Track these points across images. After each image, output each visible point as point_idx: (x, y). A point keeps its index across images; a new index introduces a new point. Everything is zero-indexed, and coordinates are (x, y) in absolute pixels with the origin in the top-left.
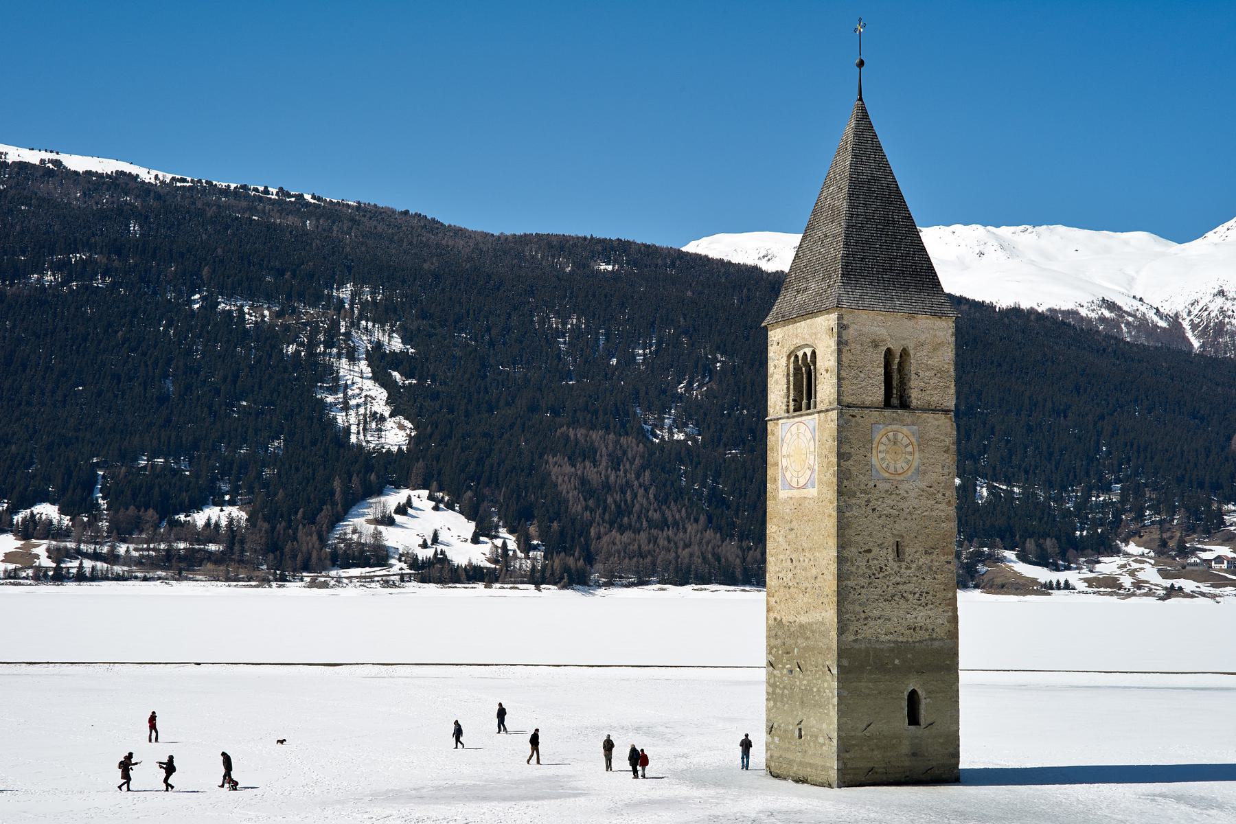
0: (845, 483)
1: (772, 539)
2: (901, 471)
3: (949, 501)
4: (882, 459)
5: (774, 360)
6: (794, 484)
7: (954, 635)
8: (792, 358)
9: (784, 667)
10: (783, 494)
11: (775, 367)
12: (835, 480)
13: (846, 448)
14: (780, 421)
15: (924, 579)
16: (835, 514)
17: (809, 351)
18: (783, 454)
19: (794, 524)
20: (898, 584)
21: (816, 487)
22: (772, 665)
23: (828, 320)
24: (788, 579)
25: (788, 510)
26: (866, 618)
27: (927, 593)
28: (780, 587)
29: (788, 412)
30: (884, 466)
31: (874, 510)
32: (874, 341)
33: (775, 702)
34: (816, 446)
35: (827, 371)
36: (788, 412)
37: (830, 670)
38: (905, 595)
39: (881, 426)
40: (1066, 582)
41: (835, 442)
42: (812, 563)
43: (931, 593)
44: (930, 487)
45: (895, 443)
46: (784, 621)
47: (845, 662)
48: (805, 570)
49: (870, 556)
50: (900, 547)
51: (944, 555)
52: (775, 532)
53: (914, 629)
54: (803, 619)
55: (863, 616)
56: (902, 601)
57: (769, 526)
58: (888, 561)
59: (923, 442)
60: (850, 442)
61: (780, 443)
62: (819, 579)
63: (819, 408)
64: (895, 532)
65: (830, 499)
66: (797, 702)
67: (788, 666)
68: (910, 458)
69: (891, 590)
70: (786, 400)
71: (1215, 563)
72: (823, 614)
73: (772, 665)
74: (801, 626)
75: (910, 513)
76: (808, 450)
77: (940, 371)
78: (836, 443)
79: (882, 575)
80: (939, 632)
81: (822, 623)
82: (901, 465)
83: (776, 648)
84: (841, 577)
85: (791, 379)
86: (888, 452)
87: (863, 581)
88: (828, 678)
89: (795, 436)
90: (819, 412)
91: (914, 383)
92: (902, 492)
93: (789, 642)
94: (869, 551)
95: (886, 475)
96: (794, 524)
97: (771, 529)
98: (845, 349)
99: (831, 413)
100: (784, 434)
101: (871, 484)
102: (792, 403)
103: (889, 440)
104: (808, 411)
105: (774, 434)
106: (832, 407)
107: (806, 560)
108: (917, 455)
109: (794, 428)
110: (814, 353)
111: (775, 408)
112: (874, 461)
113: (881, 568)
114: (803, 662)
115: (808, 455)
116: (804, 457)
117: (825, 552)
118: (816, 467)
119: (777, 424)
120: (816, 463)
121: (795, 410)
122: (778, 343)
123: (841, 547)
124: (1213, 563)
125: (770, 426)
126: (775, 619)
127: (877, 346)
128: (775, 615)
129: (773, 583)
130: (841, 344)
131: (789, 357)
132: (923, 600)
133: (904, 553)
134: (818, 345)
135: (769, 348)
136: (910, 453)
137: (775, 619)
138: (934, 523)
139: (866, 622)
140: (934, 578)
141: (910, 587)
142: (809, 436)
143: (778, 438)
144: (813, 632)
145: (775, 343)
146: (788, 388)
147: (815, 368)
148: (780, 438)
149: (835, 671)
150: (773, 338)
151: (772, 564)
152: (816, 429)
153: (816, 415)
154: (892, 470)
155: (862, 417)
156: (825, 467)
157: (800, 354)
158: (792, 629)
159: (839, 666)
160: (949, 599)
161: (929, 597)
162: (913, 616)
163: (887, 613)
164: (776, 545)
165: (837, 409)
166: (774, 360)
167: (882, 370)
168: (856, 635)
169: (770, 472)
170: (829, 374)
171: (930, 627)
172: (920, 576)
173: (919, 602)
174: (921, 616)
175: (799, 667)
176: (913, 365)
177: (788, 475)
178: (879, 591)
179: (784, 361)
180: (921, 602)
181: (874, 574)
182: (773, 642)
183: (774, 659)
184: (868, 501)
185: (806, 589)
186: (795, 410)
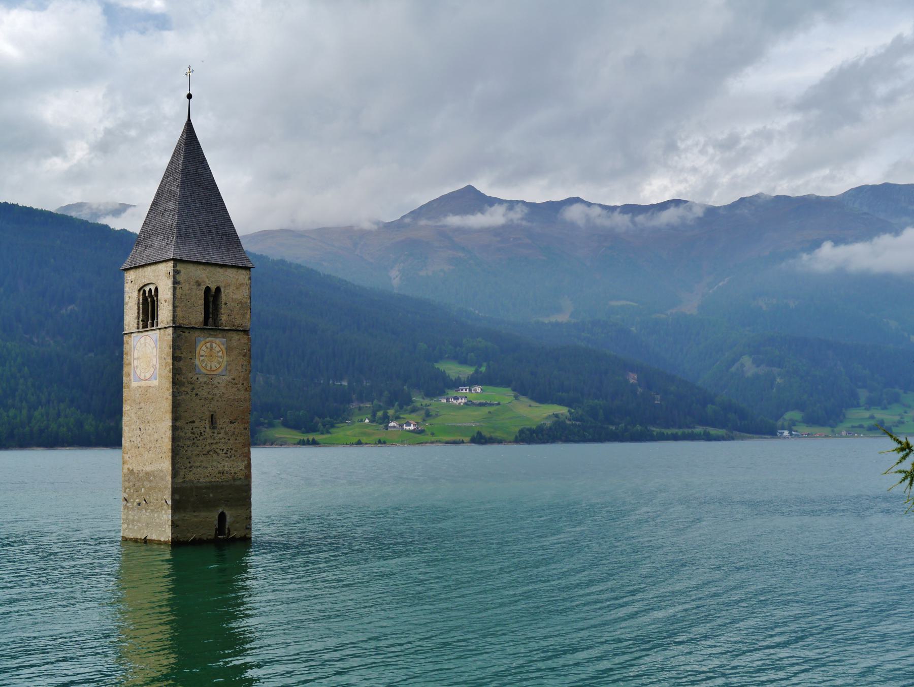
0: (178, 376)
2: (215, 369)
3: (246, 388)
4: (203, 361)
5: (129, 293)
6: (142, 378)
7: (248, 477)
8: (141, 292)
9: (134, 502)
10: (134, 384)
11: (130, 297)
12: (171, 375)
13: (178, 354)
14: (133, 334)
15: (229, 440)
16: (170, 397)
18: (135, 357)
19: (142, 405)
20: (212, 443)
22: (126, 500)
24: (138, 442)
25: (138, 395)
26: (191, 467)
27: (231, 449)
28: (132, 447)
29: (138, 328)
30: (204, 365)
31: (197, 394)
32: (197, 282)
33: (128, 525)
35: (166, 301)
36: (138, 328)
37: (166, 502)
38: (216, 450)
39: (202, 339)
40: (313, 440)
41: (170, 349)
42: (154, 430)
43: (234, 449)
44: (234, 379)
45: (211, 350)
46: (135, 470)
47: (177, 497)
48: (150, 435)
49: (195, 425)
50: (214, 419)
51: (242, 424)
53: (223, 473)
54: (148, 468)
55: (189, 465)
56: (215, 456)
57: (124, 406)
58: (206, 428)
59: (229, 349)
60: (181, 349)
62: (159, 441)
63: (159, 326)
64: (211, 409)
66: (143, 523)
67: (137, 500)
68: (221, 360)
69: (208, 448)
70: (137, 320)
71: (406, 426)
73: (126, 500)
74: (147, 473)
75: (221, 397)
77: (241, 303)
78: (171, 350)
79: (202, 438)
80: (240, 475)
81: (161, 471)
82: (214, 365)
84: (174, 439)
85: (141, 306)
86: (206, 356)
87: (189, 443)
88: (165, 507)
90: (160, 329)
91: (223, 310)
92: (215, 382)
94: (194, 422)
95: (205, 372)
96: (142, 405)
97: (126, 408)
98: (178, 287)
99: (168, 330)
100: (135, 343)
101: (195, 378)
102: (141, 323)
103: (207, 348)
104: (153, 328)
105: (128, 344)
106: (169, 325)
107: (150, 428)
108: (225, 358)
109: (142, 340)
110: (156, 289)
111: (129, 326)
112: (197, 362)
113: (201, 433)
114: (148, 497)
116: (149, 359)
118: (158, 366)
119: (130, 337)
120: (158, 363)
121: (143, 328)
122: (132, 282)
123: (175, 419)
124: (405, 425)
125: (126, 338)
126: (128, 469)
127: (199, 285)
128: (128, 466)
129: (127, 445)
130: (175, 283)
131: (139, 291)
132: (229, 454)
133: (216, 423)
135: (126, 285)
136: (221, 357)
137: (128, 469)
138: (236, 404)
139: (191, 469)
140: (236, 439)
141: (222, 446)
142: (153, 345)
144: (155, 477)
145: (129, 282)
146: (138, 313)
147: (157, 299)
148: (132, 347)
149: (170, 503)
151: (127, 431)
152: (158, 340)
153: (158, 331)
154: (208, 368)
155: (189, 333)
156: (164, 365)
157: (147, 289)
158: (140, 475)
159: (172, 499)
160: (246, 453)
161: (233, 452)
162: (222, 465)
163: (204, 464)
165: (173, 327)
166: (129, 293)
167: (202, 302)
168: (184, 478)
169: (125, 369)
170: (167, 303)
171: (233, 471)
172: (227, 438)
173: (226, 455)
174: (226, 465)
175: (145, 501)
176: (223, 297)
177: (138, 372)
178: (199, 449)
179: (135, 294)
180: (227, 455)
181: (196, 437)
182: (127, 484)
183: (127, 496)
184: (193, 389)
186: (143, 328)
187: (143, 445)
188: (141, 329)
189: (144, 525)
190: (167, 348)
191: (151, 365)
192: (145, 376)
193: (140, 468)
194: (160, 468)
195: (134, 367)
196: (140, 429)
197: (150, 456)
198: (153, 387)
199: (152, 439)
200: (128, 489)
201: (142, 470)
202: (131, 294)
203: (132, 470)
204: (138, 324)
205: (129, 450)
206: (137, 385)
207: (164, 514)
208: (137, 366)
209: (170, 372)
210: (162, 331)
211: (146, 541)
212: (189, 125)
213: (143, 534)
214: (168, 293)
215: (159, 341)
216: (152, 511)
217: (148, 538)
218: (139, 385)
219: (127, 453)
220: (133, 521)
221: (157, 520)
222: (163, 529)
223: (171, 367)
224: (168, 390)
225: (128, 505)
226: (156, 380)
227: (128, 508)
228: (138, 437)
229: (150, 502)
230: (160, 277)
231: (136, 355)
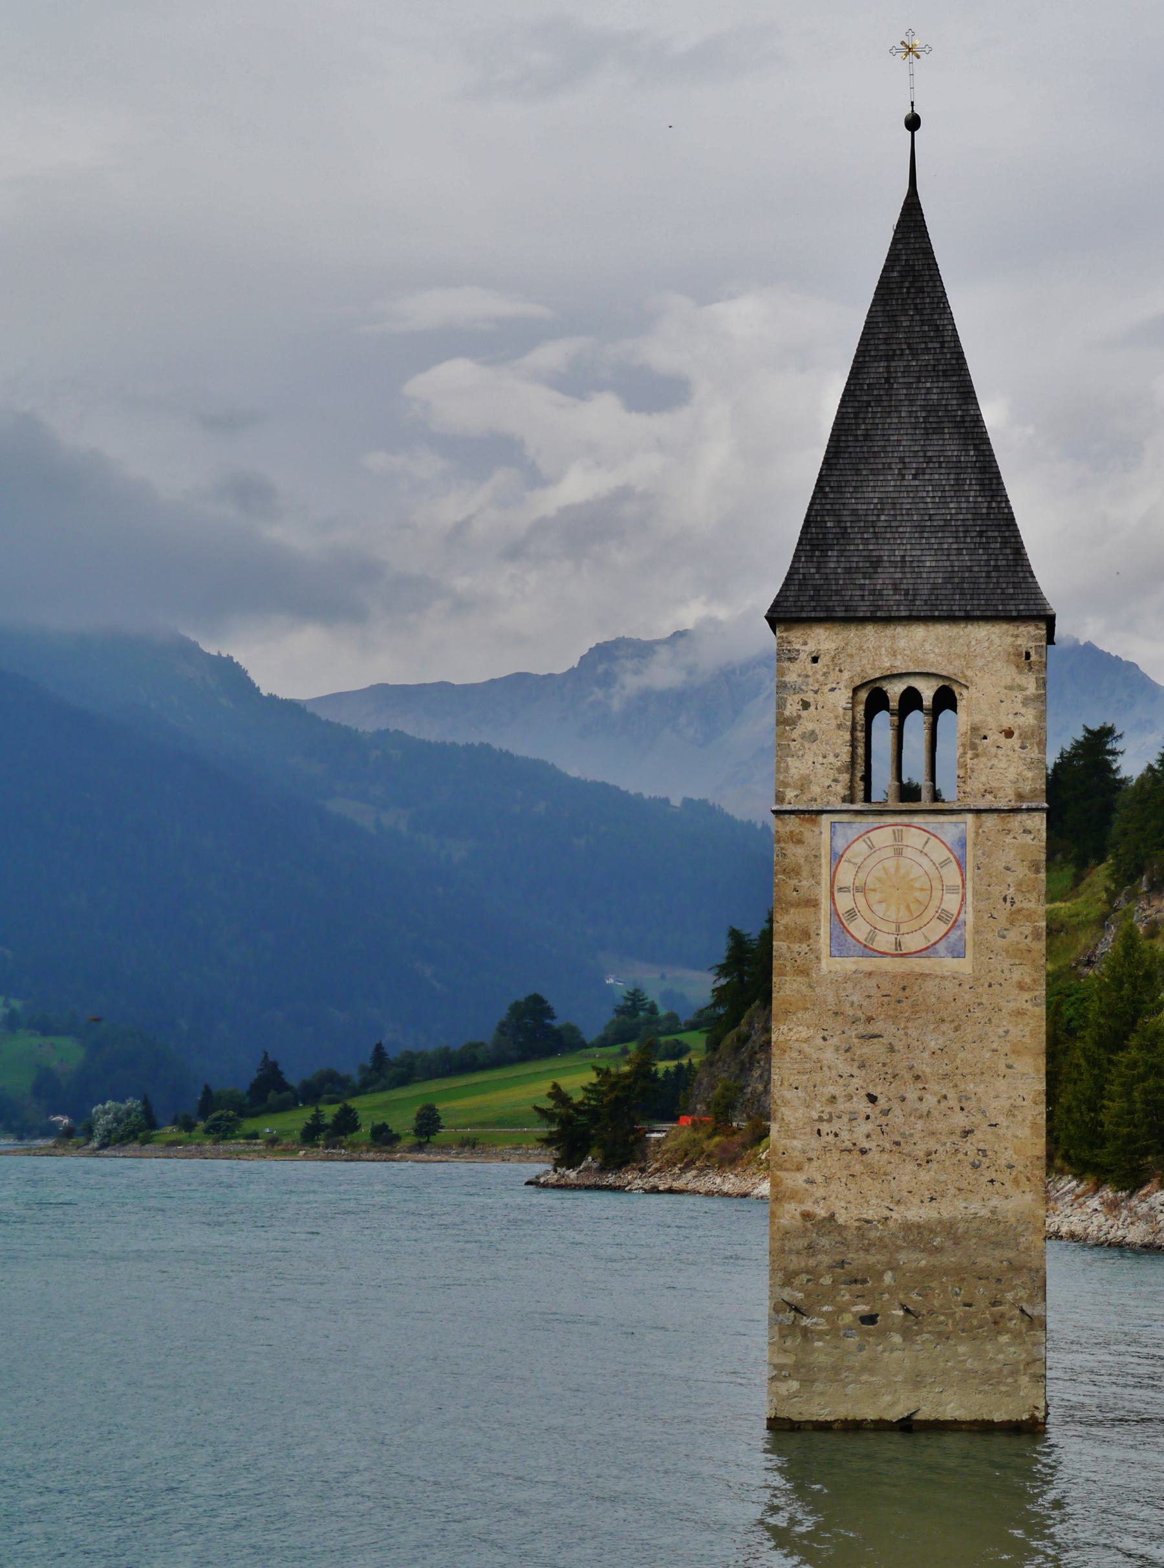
1: (794, 1055)
6: (884, 942)
8: (863, 695)
9: (841, 1310)
10: (829, 965)
11: (806, 705)
14: (824, 816)
16: (1041, 1011)
17: (927, 691)
18: (837, 885)
21: (969, 952)
23: (1017, 636)
28: (826, 1149)
33: (807, 1382)
34: (969, 875)
41: (1037, 871)
52: (806, 1040)
54: (916, 1213)
61: (825, 861)
62: (978, 1134)
65: (1020, 983)
67: (862, 1308)
70: (846, 777)
72: (994, 1202)
73: (797, 1310)
74: (908, 1227)
76: (937, 884)
78: (1043, 875)
83: (808, 1272)
89: (890, 852)
90: (978, 812)
93: (858, 1259)
99: (1016, 821)
114: (915, 1297)
115: (937, 894)
117: (1001, 1085)
118: (969, 917)
120: (969, 908)
122: (815, 660)
126: (806, 1216)
128: (808, 1207)
131: (856, 690)
134: (976, 679)
143: (818, 847)
146: (853, 755)
148: (825, 851)
150: (797, 647)
153: (969, 817)
157: (894, 690)
158: (873, 1234)
164: (807, 1066)
170: (1015, 741)
177: (859, 929)
179: (843, 697)
182: (795, 1262)
183: (801, 1295)
185: (929, 1154)
187: (888, 1146)
188: (857, 806)
189: (900, 1378)
190: (1022, 871)
191: (931, 911)
192: (898, 944)
193: (869, 1214)
194: (984, 1213)
195: (835, 912)
196: (872, 1099)
197: (925, 1176)
198: (943, 978)
199: (941, 1126)
200: (804, 1277)
201: (886, 1219)
202: (811, 694)
203: (832, 1216)
204: (851, 788)
205: (810, 1160)
206: (853, 968)
207: (1009, 1344)
208: (852, 914)
209: (1036, 936)
210: (990, 821)
211: (907, 1426)
212: (912, 210)
213: (892, 1405)
214: (1023, 711)
215: (975, 844)
216: (942, 1336)
217: (918, 1417)
218: (870, 969)
219: (799, 1169)
220: (836, 1369)
221: (970, 1364)
222: (1003, 1389)
223: (1044, 924)
224: (1021, 987)
225: (805, 1322)
226: (960, 955)
227: (805, 1331)
228: (861, 1120)
229: (931, 1312)
230: (980, 662)
231: (846, 875)
